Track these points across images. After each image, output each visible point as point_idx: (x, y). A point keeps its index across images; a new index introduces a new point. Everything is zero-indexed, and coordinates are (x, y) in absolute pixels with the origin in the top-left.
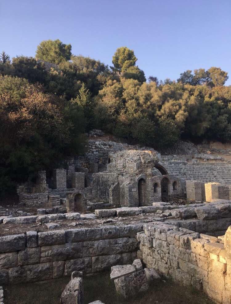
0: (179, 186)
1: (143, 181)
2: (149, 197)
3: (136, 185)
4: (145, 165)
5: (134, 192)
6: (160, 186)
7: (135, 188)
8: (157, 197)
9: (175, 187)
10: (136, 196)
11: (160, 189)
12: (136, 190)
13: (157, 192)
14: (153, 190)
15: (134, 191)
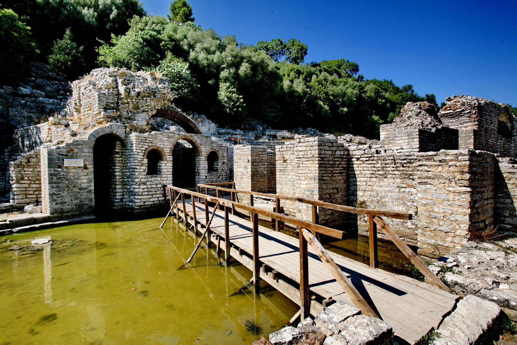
0: (223, 163)
1: (118, 142)
2: (132, 185)
3: (86, 150)
4: (128, 103)
5: (73, 170)
6: (170, 158)
7: (80, 157)
8: (157, 184)
9: (216, 164)
10: (86, 180)
11: (170, 165)
12: (82, 165)
13: (160, 172)
14: (144, 168)
15: (76, 165)
